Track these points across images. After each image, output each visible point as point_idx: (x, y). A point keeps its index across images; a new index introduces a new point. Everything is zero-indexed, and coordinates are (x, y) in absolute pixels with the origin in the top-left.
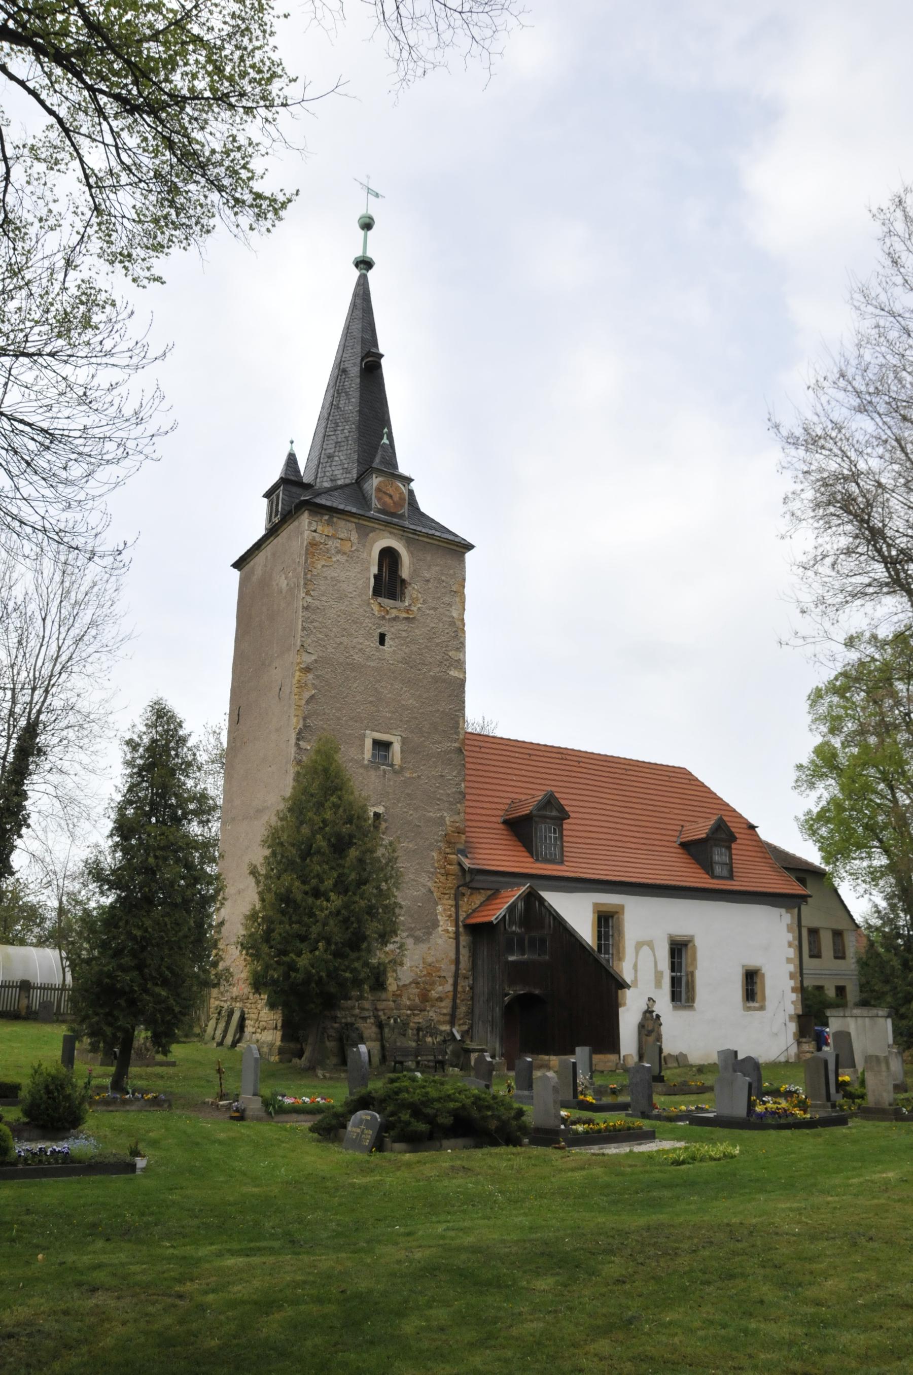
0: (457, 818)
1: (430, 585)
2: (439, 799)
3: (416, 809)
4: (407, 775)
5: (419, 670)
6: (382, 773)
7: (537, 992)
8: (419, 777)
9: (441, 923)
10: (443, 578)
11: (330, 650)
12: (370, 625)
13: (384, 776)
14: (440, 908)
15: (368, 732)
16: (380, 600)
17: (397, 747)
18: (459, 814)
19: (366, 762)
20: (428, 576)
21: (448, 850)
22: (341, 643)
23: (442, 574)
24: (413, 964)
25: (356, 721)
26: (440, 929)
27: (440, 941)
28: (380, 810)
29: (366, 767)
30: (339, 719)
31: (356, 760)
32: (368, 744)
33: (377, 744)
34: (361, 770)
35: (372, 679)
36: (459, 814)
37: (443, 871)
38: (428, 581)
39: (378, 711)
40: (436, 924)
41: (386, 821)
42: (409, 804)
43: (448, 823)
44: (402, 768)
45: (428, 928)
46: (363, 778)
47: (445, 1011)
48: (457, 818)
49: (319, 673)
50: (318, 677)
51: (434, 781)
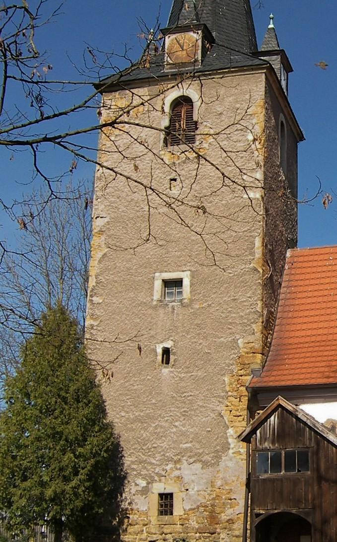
0: (251, 338)
1: (223, 117)
2: (231, 323)
3: (205, 338)
4: (197, 306)
5: (211, 202)
6: (170, 309)
7: (294, 511)
8: (209, 306)
9: (232, 446)
10: (238, 106)
11: (122, 208)
12: (160, 175)
13: (173, 312)
14: (231, 431)
15: (157, 274)
16: (170, 148)
17: (186, 282)
18: (253, 334)
19: (155, 303)
20: (220, 110)
21: (242, 372)
22: (132, 200)
23: (237, 102)
24: (200, 488)
25: (146, 267)
26: (231, 451)
27: (230, 464)
28: (169, 344)
29: (155, 308)
30: (129, 269)
31: (145, 303)
32: (158, 284)
33: (167, 283)
34: (150, 311)
35: (161, 224)
36: (253, 334)
37: (235, 394)
38: (221, 114)
39: (168, 253)
40: (226, 447)
41: (174, 354)
42: (199, 334)
43: (241, 345)
44: (192, 301)
45: (217, 451)
46: (152, 318)
47: (237, 533)
48: (251, 338)
49: (112, 232)
50: (110, 236)
51: (225, 306)
